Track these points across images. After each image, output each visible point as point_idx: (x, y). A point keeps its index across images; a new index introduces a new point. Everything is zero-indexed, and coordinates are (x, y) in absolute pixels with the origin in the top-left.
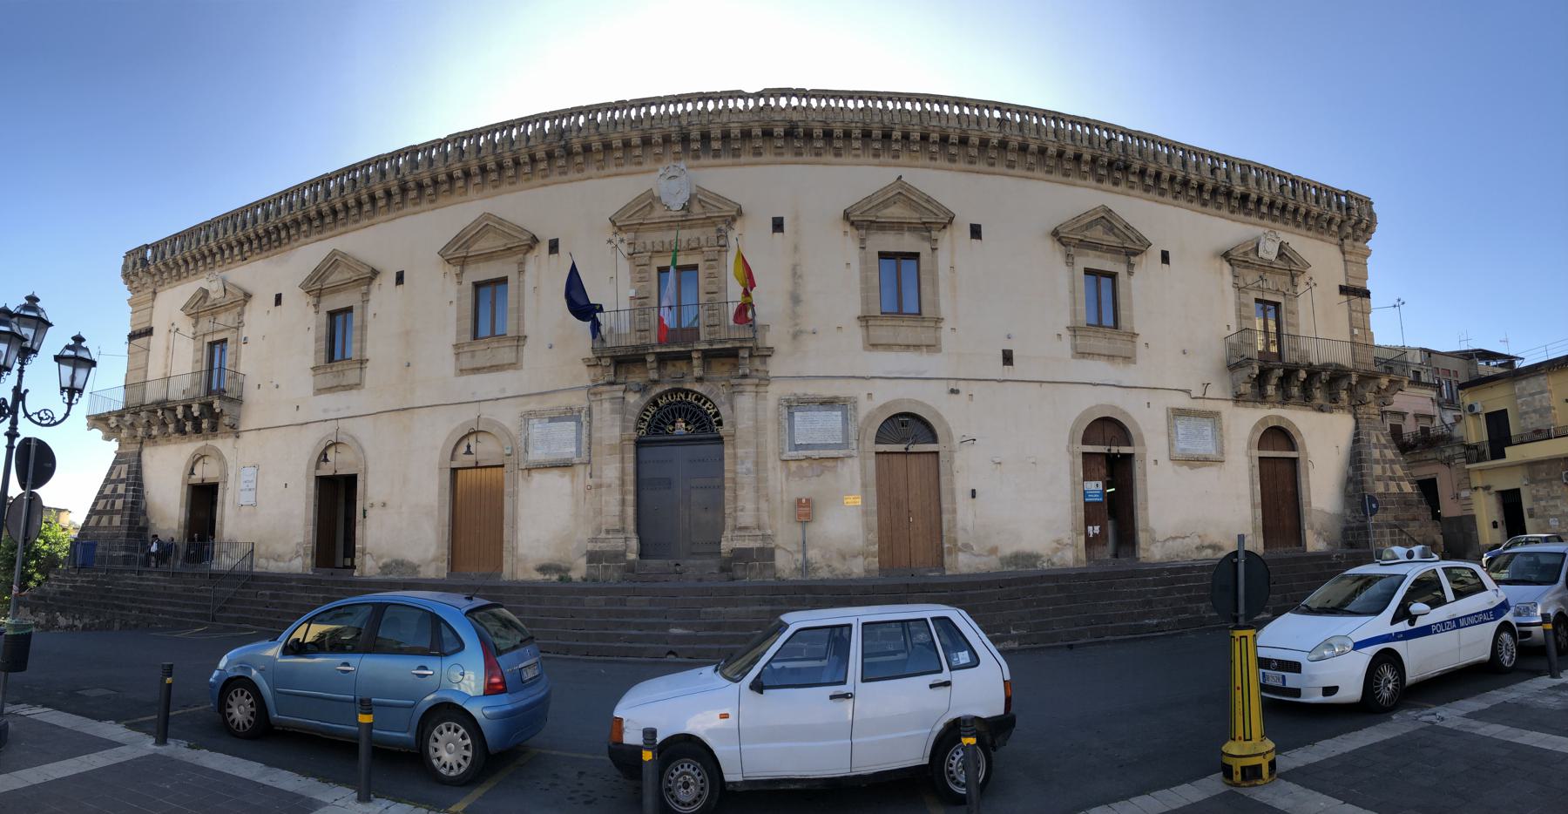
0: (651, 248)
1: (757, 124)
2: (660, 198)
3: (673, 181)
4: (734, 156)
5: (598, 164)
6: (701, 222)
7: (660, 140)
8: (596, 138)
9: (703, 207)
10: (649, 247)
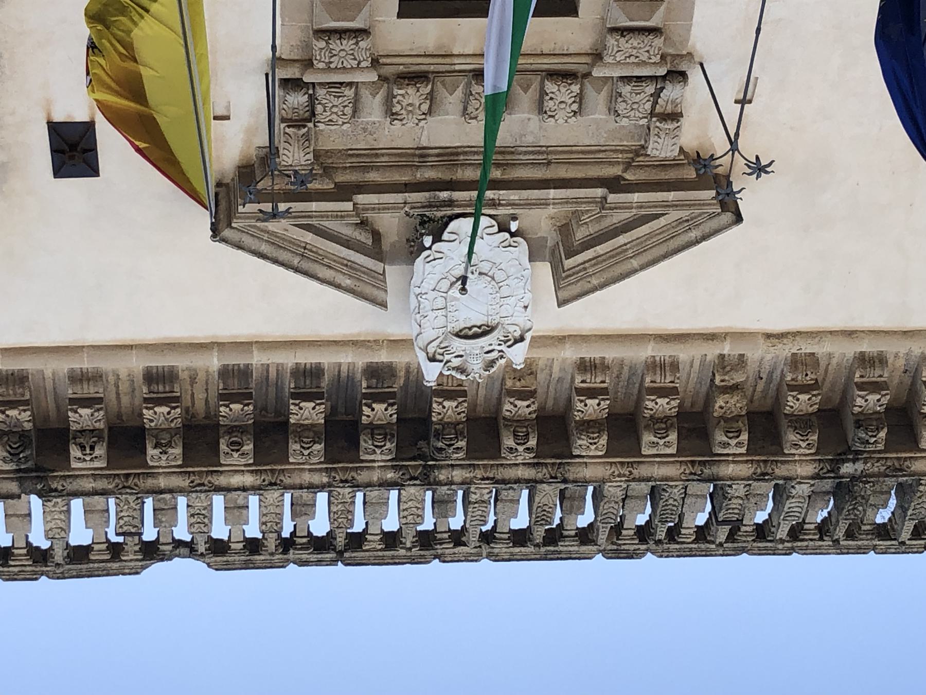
0: (590, 91)
1: (162, 482)
2: (533, 257)
3: (477, 318)
4: (245, 373)
5: (738, 378)
6: (374, 176)
7: (508, 441)
8: (730, 470)
9: (363, 224)
10: (597, 100)
